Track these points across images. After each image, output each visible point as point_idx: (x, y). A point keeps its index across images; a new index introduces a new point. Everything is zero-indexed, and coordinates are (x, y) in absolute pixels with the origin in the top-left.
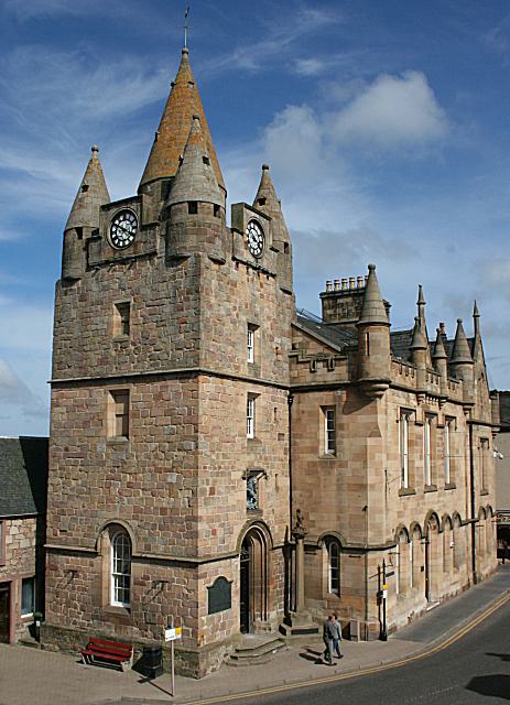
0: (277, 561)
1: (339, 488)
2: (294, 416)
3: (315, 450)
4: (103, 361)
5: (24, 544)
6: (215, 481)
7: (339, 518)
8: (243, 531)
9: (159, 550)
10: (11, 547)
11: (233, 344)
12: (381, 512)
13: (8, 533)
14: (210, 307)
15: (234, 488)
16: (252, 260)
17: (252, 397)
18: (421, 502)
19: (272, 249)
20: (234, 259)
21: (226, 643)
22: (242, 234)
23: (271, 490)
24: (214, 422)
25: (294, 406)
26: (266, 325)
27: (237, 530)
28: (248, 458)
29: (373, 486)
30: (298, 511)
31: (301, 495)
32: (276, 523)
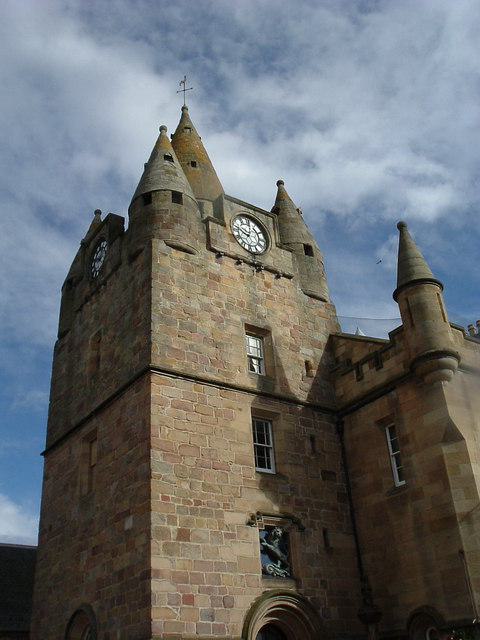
8: (255, 607)
14: (170, 296)
15: (232, 536)
16: (246, 254)
22: (224, 225)
24: (182, 437)
25: (347, 435)
27: (243, 603)
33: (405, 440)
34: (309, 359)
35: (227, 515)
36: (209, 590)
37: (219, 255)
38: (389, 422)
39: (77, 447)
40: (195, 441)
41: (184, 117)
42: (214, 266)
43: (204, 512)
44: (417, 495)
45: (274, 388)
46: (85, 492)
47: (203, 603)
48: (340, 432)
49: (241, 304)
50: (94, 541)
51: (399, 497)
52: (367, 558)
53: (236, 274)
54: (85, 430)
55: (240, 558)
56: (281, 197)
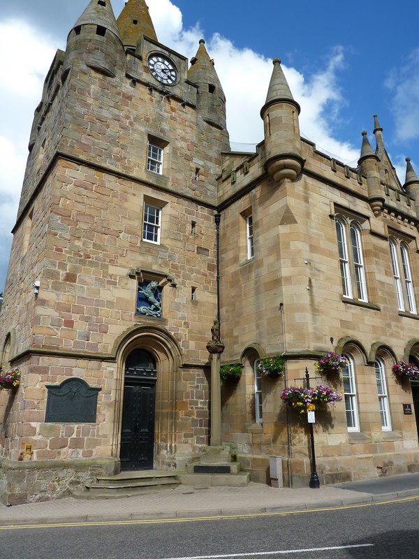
1: (258, 292)
2: (221, 234)
3: (236, 259)
7: (258, 326)
11: (123, 147)
12: (301, 309)
14: (86, 105)
17: (153, 207)
18: (393, 323)
19: (188, 82)
20: (128, 76)
21: (79, 467)
25: (221, 224)
28: (140, 258)
29: (289, 279)
31: (227, 311)
32: (192, 338)
34: (199, 167)
35: (110, 267)
36: (87, 319)
37: (135, 82)
38: (247, 214)
40: (93, 213)
42: (127, 86)
43: (91, 263)
45: (166, 184)
47: (80, 327)
49: (147, 120)
52: (223, 310)
55: (118, 299)
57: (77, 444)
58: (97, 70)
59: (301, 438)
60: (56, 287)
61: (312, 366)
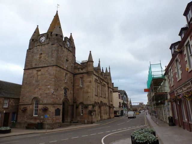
0: (70, 108)
1: (83, 93)
2: (75, 79)
3: (78, 86)
4: (36, 65)
5: (14, 104)
6: (58, 88)
9: (45, 102)
10: (11, 105)
11: (63, 62)
12: (91, 97)
13: (10, 101)
17: (66, 74)
20: (64, 46)
21: (59, 123)
23: (69, 93)
25: (75, 77)
26: (70, 61)
27: (62, 99)
29: (90, 92)
30: (75, 97)
33: (84, 81)
37: (65, 47)
38: (82, 78)
39: (35, 71)
41: (57, 13)
44: (84, 88)
46: (36, 79)
48: (74, 77)
50: (39, 88)
51: (81, 88)
52: (74, 95)
53: (66, 51)
54: (37, 69)
56: (71, 36)
57: (58, 119)
58: (61, 46)
59: (91, 117)
60: (56, 92)
61: (92, 106)
